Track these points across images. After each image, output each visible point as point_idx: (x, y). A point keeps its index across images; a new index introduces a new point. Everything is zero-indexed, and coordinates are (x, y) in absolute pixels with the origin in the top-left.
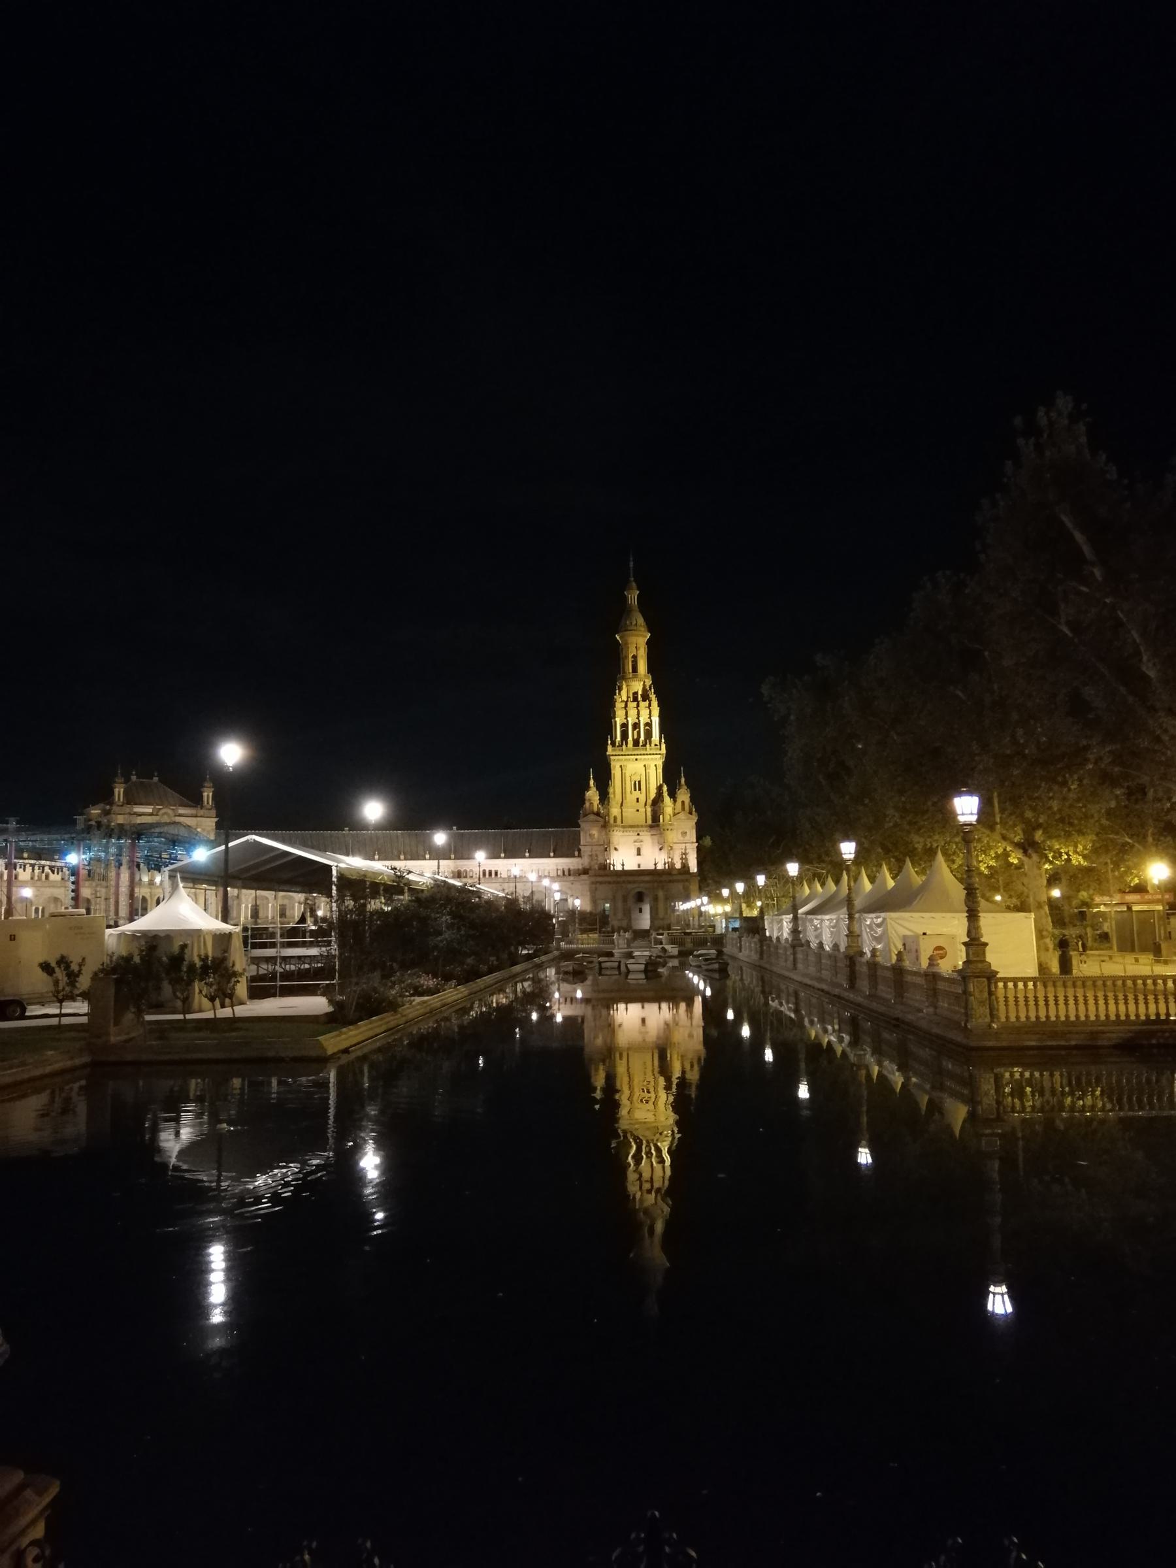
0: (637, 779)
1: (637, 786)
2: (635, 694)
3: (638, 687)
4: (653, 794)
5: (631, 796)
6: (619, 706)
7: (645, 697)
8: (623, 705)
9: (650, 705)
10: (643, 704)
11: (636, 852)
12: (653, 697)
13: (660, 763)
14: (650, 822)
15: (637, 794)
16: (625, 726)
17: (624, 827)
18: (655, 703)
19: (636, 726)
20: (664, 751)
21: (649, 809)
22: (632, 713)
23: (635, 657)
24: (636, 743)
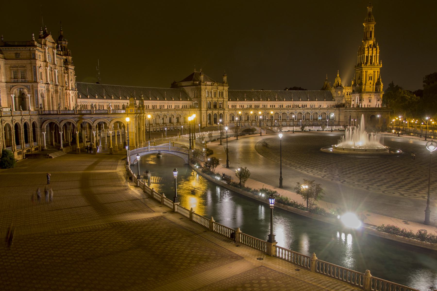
0: (371, 76)
1: (370, 78)
2: (370, 45)
3: (371, 42)
4: (376, 82)
5: (368, 82)
6: (366, 49)
7: (375, 46)
8: (367, 49)
9: (376, 50)
10: (374, 49)
11: (368, 101)
12: (378, 47)
13: (379, 70)
14: (374, 91)
15: (370, 81)
16: (367, 57)
17: (366, 92)
18: (378, 49)
19: (371, 57)
20: (381, 66)
21: (374, 86)
22: (370, 52)
23: (371, 32)
24: (371, 63)
